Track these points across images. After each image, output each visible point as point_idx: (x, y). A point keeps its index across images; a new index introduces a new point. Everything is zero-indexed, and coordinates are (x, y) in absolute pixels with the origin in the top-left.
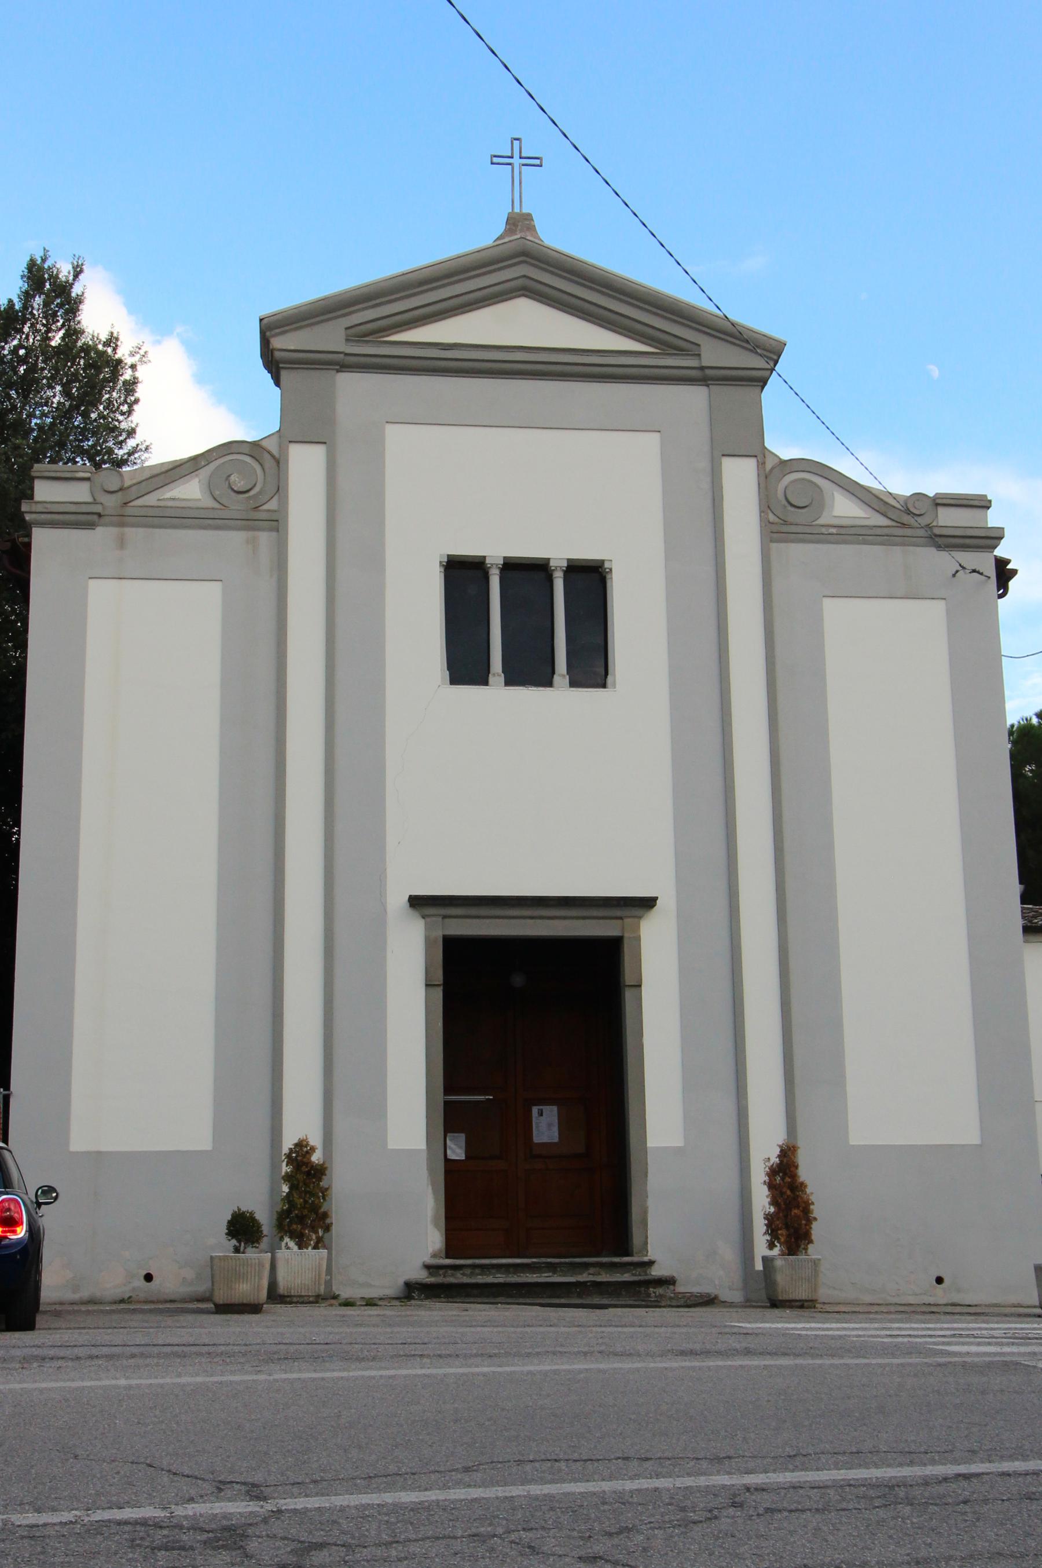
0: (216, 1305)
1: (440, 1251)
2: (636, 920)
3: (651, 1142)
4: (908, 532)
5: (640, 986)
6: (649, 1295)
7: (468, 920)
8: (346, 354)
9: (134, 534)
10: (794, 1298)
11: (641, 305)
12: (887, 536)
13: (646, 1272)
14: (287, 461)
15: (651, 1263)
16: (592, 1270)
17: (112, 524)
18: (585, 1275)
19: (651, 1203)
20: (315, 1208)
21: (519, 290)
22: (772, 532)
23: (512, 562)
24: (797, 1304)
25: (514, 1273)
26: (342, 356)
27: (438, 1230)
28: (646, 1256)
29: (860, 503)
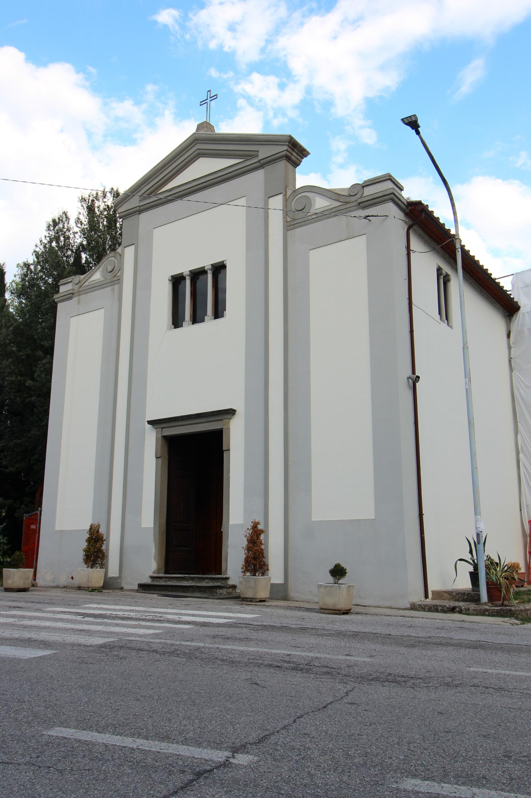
0: (5, 589)
1: (156, 570)
2: (228, 420)
3: (231, 522)
4: (348, 205)
5: (229, 450)
6: (216, 593)
7: (169, 429)
8: (140, 206)
9: (83, 297)
10: (247, 597)
11: (183, 153)
12: (339, 211)
13: (226, 582)
14: (124, 256)
15: (227, 579)
16: (206, 581)
17: (77, 296)
18: (204, 583)
19: (229, 550)
20: (100, 551)
21: (197, 156)
22: (288, 226)
23: (196, 271)
24: (249, 600)
25: (180, 581)
26: (138, 207)
27: (156, 561)
28: (227, 575)
29: (327, 198)
